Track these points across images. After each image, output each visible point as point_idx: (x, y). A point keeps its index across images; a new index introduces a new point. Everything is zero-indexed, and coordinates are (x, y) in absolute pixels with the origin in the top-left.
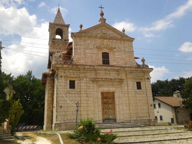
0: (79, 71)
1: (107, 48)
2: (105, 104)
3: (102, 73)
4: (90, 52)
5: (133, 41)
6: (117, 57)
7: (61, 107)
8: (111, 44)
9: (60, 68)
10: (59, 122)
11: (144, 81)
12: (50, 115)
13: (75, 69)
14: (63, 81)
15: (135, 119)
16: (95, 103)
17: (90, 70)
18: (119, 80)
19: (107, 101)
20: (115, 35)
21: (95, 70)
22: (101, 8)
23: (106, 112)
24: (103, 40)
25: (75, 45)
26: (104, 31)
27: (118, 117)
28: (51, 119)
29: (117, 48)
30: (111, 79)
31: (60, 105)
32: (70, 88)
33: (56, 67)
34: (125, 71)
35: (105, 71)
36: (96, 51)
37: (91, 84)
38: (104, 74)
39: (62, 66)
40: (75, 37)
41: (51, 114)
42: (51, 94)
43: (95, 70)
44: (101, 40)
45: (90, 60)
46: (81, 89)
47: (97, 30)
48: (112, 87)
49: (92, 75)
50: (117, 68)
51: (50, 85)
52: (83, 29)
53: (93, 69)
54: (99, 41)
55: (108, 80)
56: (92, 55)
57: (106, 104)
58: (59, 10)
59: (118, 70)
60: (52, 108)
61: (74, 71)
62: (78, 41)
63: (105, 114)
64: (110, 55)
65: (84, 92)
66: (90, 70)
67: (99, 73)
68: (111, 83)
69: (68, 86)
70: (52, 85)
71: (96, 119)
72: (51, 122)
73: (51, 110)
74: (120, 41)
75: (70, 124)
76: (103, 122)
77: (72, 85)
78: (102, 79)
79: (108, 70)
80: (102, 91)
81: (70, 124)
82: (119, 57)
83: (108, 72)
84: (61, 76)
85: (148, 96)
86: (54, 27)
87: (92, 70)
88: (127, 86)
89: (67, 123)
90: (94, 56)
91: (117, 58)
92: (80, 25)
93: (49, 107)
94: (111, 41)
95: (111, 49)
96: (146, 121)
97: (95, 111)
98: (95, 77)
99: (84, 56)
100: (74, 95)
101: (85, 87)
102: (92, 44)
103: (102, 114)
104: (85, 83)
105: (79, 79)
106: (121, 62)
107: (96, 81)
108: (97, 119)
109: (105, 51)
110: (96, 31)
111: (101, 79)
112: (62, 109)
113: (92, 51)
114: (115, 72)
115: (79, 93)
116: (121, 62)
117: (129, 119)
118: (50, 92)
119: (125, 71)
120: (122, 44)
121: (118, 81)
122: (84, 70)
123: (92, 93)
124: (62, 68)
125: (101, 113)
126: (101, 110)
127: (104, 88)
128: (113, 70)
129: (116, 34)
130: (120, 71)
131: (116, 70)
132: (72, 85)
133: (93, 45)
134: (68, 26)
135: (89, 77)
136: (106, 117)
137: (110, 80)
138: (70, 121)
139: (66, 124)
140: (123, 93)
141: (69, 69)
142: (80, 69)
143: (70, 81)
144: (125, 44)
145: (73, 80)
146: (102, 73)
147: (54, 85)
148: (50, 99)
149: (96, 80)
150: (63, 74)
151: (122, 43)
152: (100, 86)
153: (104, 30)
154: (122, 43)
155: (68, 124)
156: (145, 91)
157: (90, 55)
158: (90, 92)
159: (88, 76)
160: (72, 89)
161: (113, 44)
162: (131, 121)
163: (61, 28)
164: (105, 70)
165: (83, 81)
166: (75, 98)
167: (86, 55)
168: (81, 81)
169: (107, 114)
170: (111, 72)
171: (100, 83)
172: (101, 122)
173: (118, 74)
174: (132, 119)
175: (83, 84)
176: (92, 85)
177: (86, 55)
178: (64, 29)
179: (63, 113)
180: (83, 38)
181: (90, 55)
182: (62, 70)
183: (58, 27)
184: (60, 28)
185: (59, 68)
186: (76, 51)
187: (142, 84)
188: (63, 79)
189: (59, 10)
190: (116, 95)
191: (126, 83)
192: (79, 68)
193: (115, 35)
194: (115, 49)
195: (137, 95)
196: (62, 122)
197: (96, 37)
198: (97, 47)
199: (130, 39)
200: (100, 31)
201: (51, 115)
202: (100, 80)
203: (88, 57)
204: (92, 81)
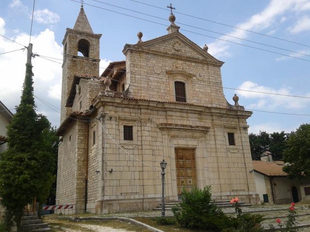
2: (180, 167)
4: (156, 79)
7: (111, 172)
9: (109, 104)
11: (239, 132)
12: (82, 187)
13: (133, 106)
14: (114, 126)
15: (228, 194)
18: (202, 129)
19: (183, 163)
20: (194, 54)
22: (171, 8)
24: (176, 61)
25: (132, 65)
26: (177, 46)
28: (84, 194)
29: (198, 76)
31: (109, 169)
32: (125, 139)
33: (102, 102)
35: (181, 112)
36: (165, 78)
37: (159, 133)
39: (113, 101)
40: (131, 52)
41: (84, 184)
42: (84, 149)
44: (173, 60)
47: (166, 43)
51: (83, 133)
52: (144, 39)
56: (159, 84)
57: (183, 168)
58: (82, 9)
59: (201, 111)
60: (85, 174)
61: (132, 110)
64: (186, 85)
65: (148, 147)
67: (171, 116)
69: (122, 135)
70: (86, 133)
72: (84, 199)
73: (84, 177)
77: (128, 134)
78: (176, 125)
79: (186, 111)
82: (201, 90)
84: (111, 118)
85: (245, 156)
86: (76, 36)
87: (161, 109)
89: (122, 200)
90: (163, 86)
92: (137, 33)
93: (80, 172)
94: (189, 63)
95: (189, 76)
96: (244, 197)
98: (165, 122)
99: (146, 85)
101: (149, 138)
103: (178, 185)
104: (149, 131)
105: (139, 124)
109: (180, 79)
112: (115, 175)
115: (140, 148)
116: (205, 99)
117: (219, 194)
118: (82, 146)
120: (206, 70)
123: (161, 148)
124: (111, 104)
125: (175, 183)
126: (175, 178)
131: (197, 112)
132: (128, 134)
134: (98, 37)
137: (189, 128)
139: (120, 202)
140: (209, 150)
141: (124, 106)
142: (141, 107)
143: (125, 127)
147: (88, 135)
148: (82, 159)
150: (112, 113)
151: (204, 68)
152: (173, 137)
153: (177, 45)
154: (204, 68)
155: (123, 202)
156: (241, 148)
157: (156, 84)
160: (129, 141)
161: (192, 68)
162: (223, 198)
163: (87, 39)
164: (180, 111)
165: (146, 128)
169: (184, 185)
174: (224, 194)
175: (147, 133)
176: (160, 135)
178: (92, 41)
180: (144, 56)
181: (156, 84)
182: (111, 108)
183: (83, 38)
184: (85, 38)
185: (107, 103)
186: (133, 76)
187: (236, 136)
188: (113, 122)
189: (82, 9)
190: (198, 153)
192: (139, 106)
194: (194, 78)
195: (230, 155)
196: (113, 198)
197: (165, 55)
200: (171, 46)
203: (152, 87)
204: (160, 128)
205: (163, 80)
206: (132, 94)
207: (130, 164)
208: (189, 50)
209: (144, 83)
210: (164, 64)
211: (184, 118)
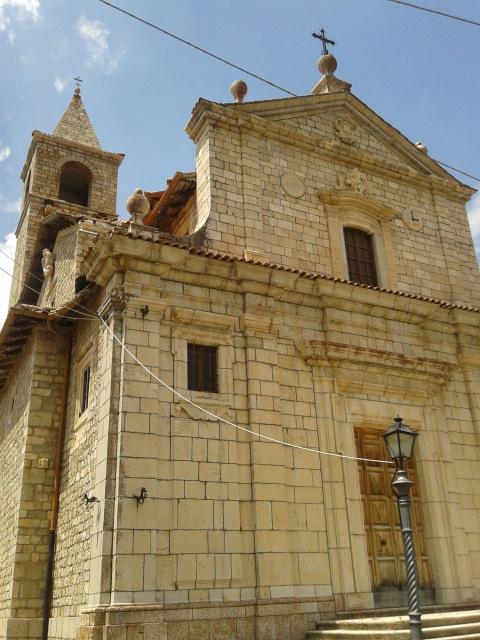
0: (239, 299)
1: (367, 209)
2: (373, 493)
3: (354, 326)
4: (289, 212)
5: (465, 199)
6: (410, 256)
7: (140, 498)
8: (378, 192)
9: (141, 265)
10: (127, 604)
12: (36, 558)
13: (217, 282)
14: (155, 340)
16: (326, 486)
17: (296, 298)
18: (435, 371)
19: (382, 478)
20: (393, 159)
21: (320, 304)
22: (325, 41)
23: (383, 543)
24: (344, 170)
25: (216, 163)
26: (346, 131)
27: (446, 575)
28: (43, 584)
29: (407, 218)
30: (403, 359)
31: (133, 488)
32: (193, 385)
33: (117, 258)
34: (453, 330)
35: (367, 314)
36: (315, 214)
37: (302, 376)
38: (365, 332)
39: (154, 256)
40: (215, 126)
41: (44, 549)
42: (51, 429)
43: (320, 304)
44: (337, 168)
45: (289, 252)
46: (253, 398)
47: (314, 118)
48: (403, 402)
49: (307, 329)
50: (422, 308)
51: (49, 379)
52: (246, 99)
53: (310, 296)
54: (328, 171)
55: (388, 363)
56: (299, 228)
57: (380, 494)
58: (77, 97)
59: (424, 317)
60: (51, 515)
61: (214, 295)
62: (233, 148)
63: (380, 555)
65: (268, 418)
66: (296, 298)
67: (339, 323)
68: (400, 382)
69: (182, 372)
70: (61, 379)
71: (342, 587)
72: (40, 603)
73: (44, 524)
74: (414, 191)
75: (196, 614)
76: (377, 599)
77: (203, 370)
78: (358, 350)
79: (380, 312)
80: (358, 420)
81: (196, 614)
82: (419, 259)
83: (379, 323)
84: (145, 311)
86: (56, 152)
87: (306, 300)
88: (465, 404)
89: (178, 607)
90: (310, 235)
91: (412, 265)
93: (31, 506)
94: (381, 181)
95: (383, 216)
97: (331, 530)
98: (320, 337)
99: (259, 226)
100: (212, 431)
101: (275, 389)
102: (300, 178)
103: (369, 555)
104: (272, 365)
105: (240, 341)
106: (431, 285)
107: (329, 359)
108: (349, 588)
110: (311, 124)
111: (356, 354)
112: (154, 513)
113: (298, 207)
114: (413, 328)
115: (242, 417)
116: (431, 285)
118: (46, 419)
119: (453, 330)
121: (431, 374)
122: (266, 295)
123: (310, 424)
124: (148, 267)
125: (361, 545)
126: (360, 527)
127: (367, 404)
128: (404, 316)
129: (398, 159)
130: (430, 324)
131: (415, 319)
132: (203, 370)
133: (303, 181)
134: (114, 161)
135: (292, 334)
136: (384, 569)
137: (397, 364)
138: (196, 597)
139: (171, 615)
141: (189, 278)
142: (246, 286)
143: (192, 347)
144: (438, 208)
146: (354, 326)
147: (68, 384)
148: (43, 461)
149: (332, 354)
150: (150, 299)
152: (349, 391)
153: (347, 128)
155: (182, 615)
157: (289, 226)
158: (300, 421)
159: (285, 331)
160: (206, 394)
161: (388, 195)
163: (86, 163)
164: (366, 309)
165: (262, 355)
166: (222, 449)
167: (273, 222)
168: (251, 352)
169: (387, 554)
170: (394, 325)
171: (349, 373)
172: (368, 602)
173: (425, 341)
175: (263, 372)
176: (305, 379)
177: (273, 222)
178: (100, 171)
179: (156, 542)
180: (254, 142)
181: (289, 226)
182: (146, 279)
183: (74, 159)
184: (82, 161)
185: (133, 264)
186: (220, 193)
188: (153, 327)
189: (77, 97)
191: (461, 388)
192: (240, 282)
193: (393, 159)
194: (398, 223)
196: (146, 600)
197: (313, 148)
198: (319, 197)
199: (459, 188)
200: (331, 130)
201: (44, 557)
202: (352, 357)
203: (278, 232)
205: (311, 217)
206: (216, 245)
207: (209, 472)
208: (378, 146)
209: (255, 217)
210: (312, 172)
211: (378, 335)
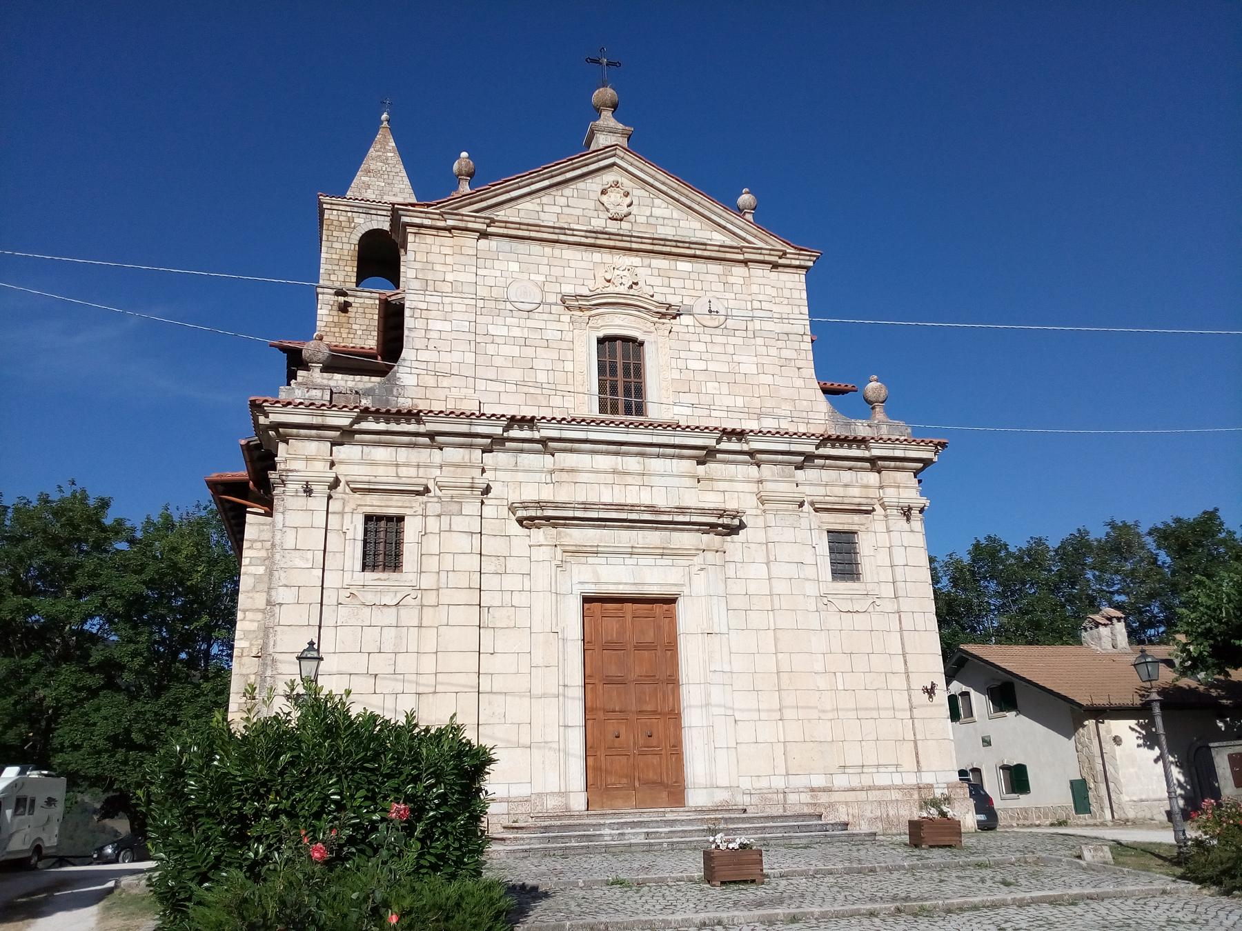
4: (516, 332)
8: (658, 281)
11: (880, 526)
15: (818, 781)
54: (583, 264)
56: (529, 352)
62: (441, 259)
64: (649, 352)
82: (712, 366)
85: (907, 623)
86: (350, 220)
96: (895, 795)
99: (470, 358)
100: (389, 616)
109: (620, 324)
110: (562, 201)
113: (530, 323)
116: (729, 401)
117: (779, 783)
120: (737, 288)
123: (518, 599)
140: (736, 603)
145: (391, 507)
151: (731, 279)
154: (731, 279)
156: (888, 591)
157: (515, 351)
161: (674, 283)
162: (792, 798)
174: (798, 782)
177: (491, 349)
181: (515, 351)
182: (312, 448)
183: (375, 225)
187: (865, 545)
190: (687, 617)
195: (834, 621)
203: (498, 361)
204: (520, 521)
205: (549, 335)
206: (410, 392)
207: (380, 664)
208: (666, 213)
209: (466, 347)
210: (556, 271)
211: (629, 479)
